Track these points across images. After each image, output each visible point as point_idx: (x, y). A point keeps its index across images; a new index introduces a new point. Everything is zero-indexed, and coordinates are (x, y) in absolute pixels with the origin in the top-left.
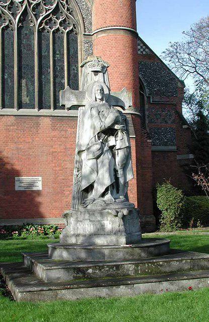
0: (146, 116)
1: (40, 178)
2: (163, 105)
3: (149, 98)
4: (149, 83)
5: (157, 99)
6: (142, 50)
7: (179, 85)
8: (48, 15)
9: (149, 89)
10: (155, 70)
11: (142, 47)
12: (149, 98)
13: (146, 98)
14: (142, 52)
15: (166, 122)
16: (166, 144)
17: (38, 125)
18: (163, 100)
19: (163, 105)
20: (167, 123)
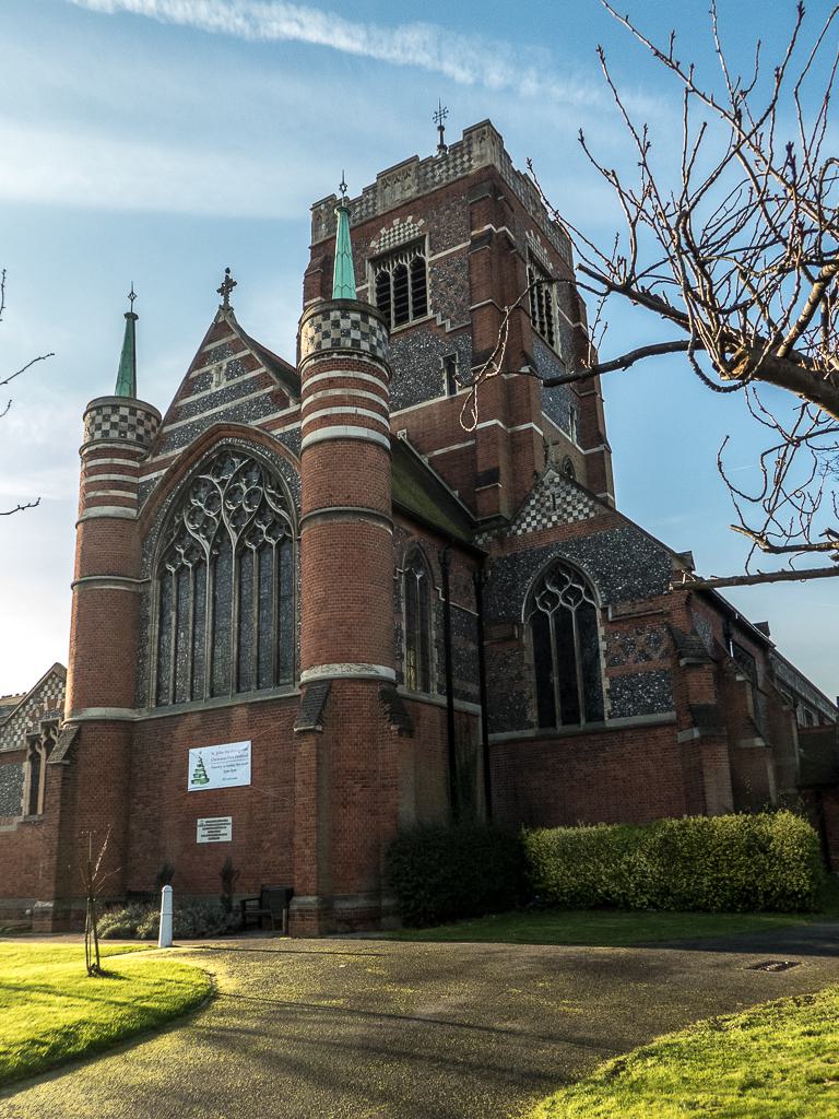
0: (602, 654)
1: (230, 819)
2: (637, 620)
3: (604, 610)
4: (604, 578)
5: (624, 608)
6: (586, 510)
7: (676, 566)
8: (252, 521)
9: (605, 591)
10: (617, 547)
11: (586, 505)
12: (604, 610)
13: (599, 613)
14: (587, 515)
15: (648, 658)
16: (649, 710)
17: (229, 720)
18: (638, 608)
19: (637, 620)
20: (651, 659)
